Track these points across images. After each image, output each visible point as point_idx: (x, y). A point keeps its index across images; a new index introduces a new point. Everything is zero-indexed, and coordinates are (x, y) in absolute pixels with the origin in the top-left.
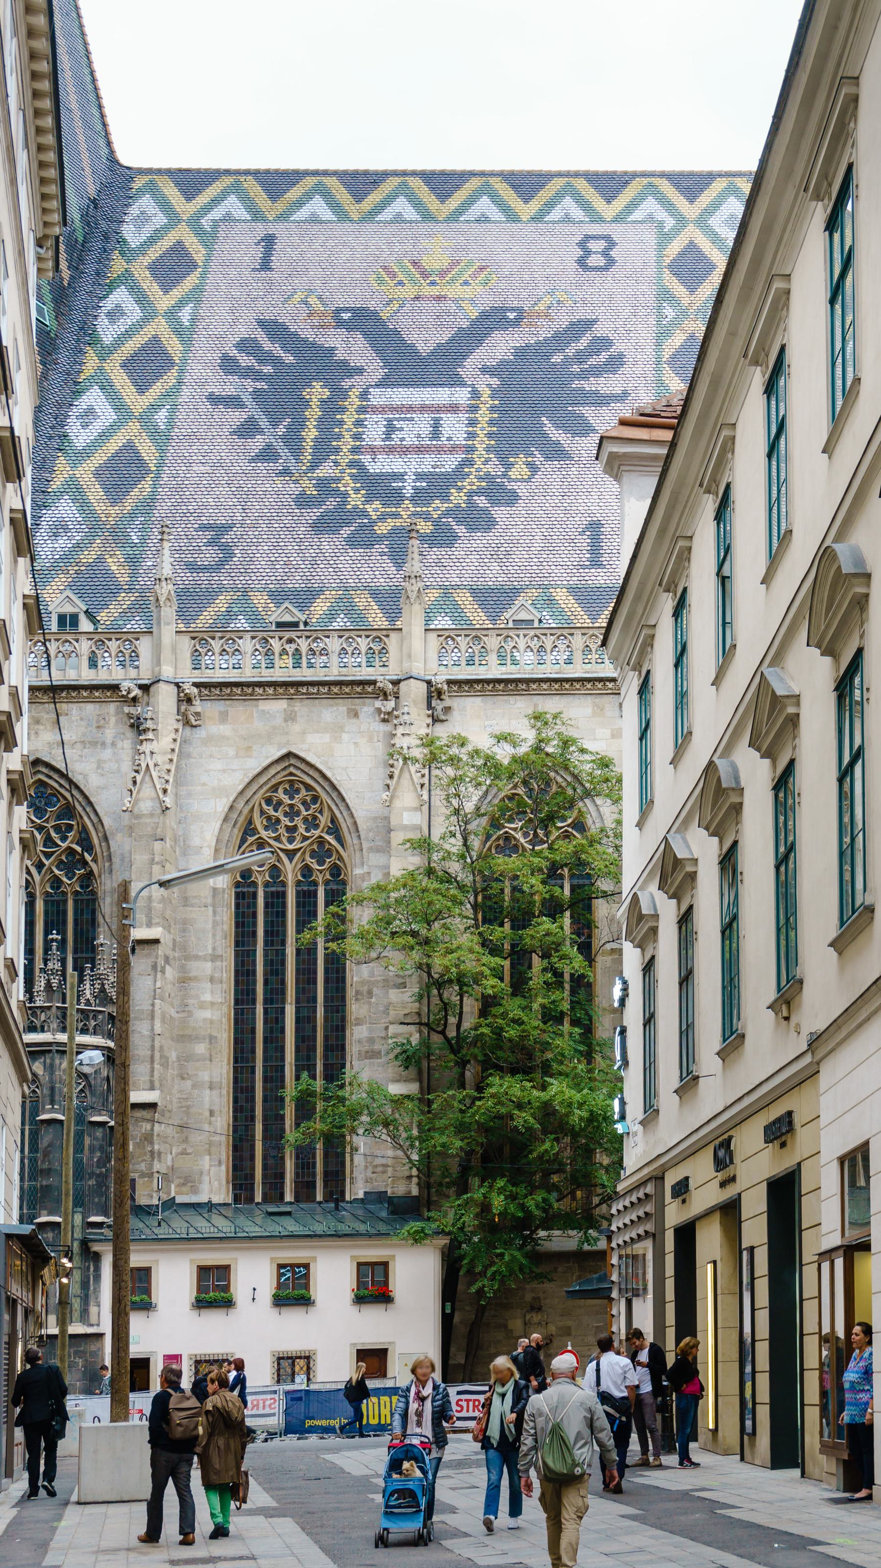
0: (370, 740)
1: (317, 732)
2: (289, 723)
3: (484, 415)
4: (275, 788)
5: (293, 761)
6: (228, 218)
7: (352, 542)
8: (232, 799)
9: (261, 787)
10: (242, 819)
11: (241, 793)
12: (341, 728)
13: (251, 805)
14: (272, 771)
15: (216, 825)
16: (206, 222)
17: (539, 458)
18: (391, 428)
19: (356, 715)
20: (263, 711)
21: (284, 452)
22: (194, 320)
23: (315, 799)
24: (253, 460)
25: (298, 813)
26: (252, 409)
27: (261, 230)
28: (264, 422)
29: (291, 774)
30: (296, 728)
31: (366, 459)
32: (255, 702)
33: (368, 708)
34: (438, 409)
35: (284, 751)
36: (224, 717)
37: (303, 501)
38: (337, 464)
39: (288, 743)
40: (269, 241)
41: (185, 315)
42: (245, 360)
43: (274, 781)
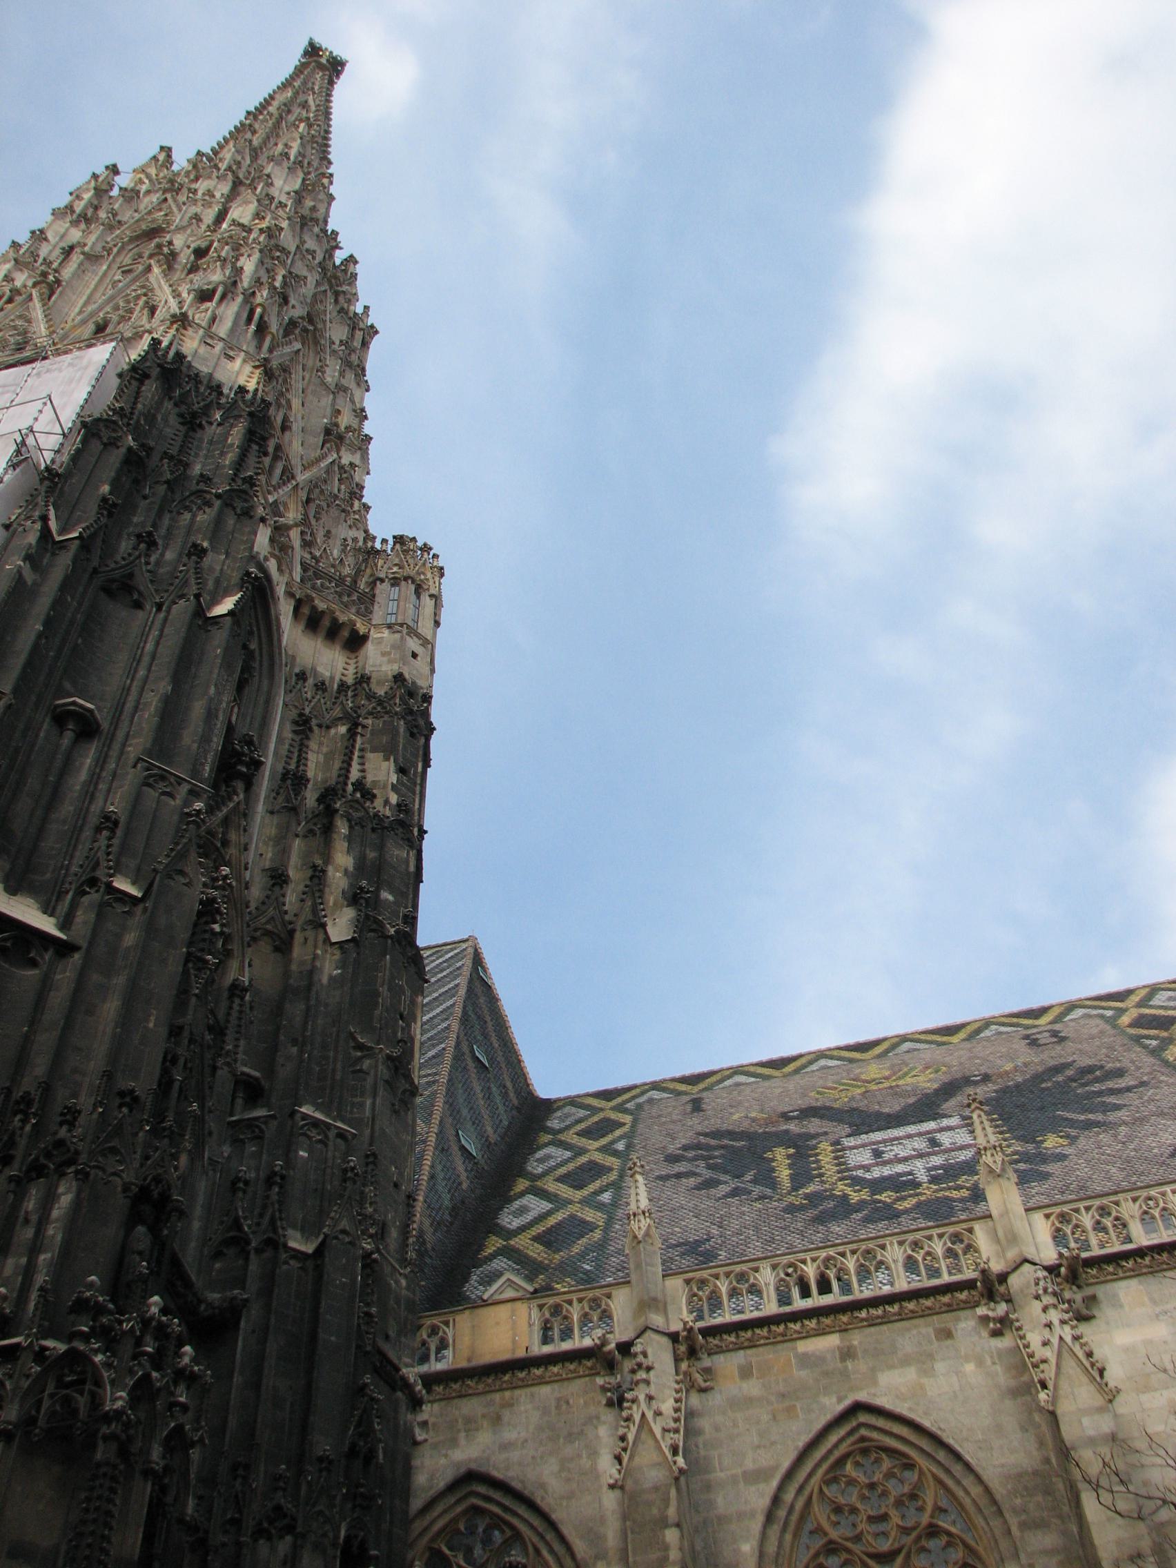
0: (980, 1363)
1: (891, 1367)
2: (849, 1364)
4: (841, 1462)
5: (863, 1418)
6: (650, 1101)
7: (867, 1220)
8: (775, 1483)
9: (818, 1465)
10: (794, 1517)
12: (931, 1356)
13: (806, 1492)
14: (833, 1438)
15: (756, 1525)
16: (628, 1106)
17: (1073, 1132)
18: (877, 1154)
19: (947, 1334)
20: (805, 1355)
21: (757, 1190)
22: (629, 1146)
23: (910, 1466)
24: (720, 1199)
25: (885, 1494)
26: (708, 1174)
28: (723, 1178)
30: (858, 1367)
31: (860, 1173)
32: (789, 1344)
33: (965, 1324)
35: (847, 1402)
36: (746, 1372)
37: (791, 1209)
38: (822, 1182)
39: (852, 1389)
41: (620, 1146)
42: (691, 1154)
43: (837, 1454)
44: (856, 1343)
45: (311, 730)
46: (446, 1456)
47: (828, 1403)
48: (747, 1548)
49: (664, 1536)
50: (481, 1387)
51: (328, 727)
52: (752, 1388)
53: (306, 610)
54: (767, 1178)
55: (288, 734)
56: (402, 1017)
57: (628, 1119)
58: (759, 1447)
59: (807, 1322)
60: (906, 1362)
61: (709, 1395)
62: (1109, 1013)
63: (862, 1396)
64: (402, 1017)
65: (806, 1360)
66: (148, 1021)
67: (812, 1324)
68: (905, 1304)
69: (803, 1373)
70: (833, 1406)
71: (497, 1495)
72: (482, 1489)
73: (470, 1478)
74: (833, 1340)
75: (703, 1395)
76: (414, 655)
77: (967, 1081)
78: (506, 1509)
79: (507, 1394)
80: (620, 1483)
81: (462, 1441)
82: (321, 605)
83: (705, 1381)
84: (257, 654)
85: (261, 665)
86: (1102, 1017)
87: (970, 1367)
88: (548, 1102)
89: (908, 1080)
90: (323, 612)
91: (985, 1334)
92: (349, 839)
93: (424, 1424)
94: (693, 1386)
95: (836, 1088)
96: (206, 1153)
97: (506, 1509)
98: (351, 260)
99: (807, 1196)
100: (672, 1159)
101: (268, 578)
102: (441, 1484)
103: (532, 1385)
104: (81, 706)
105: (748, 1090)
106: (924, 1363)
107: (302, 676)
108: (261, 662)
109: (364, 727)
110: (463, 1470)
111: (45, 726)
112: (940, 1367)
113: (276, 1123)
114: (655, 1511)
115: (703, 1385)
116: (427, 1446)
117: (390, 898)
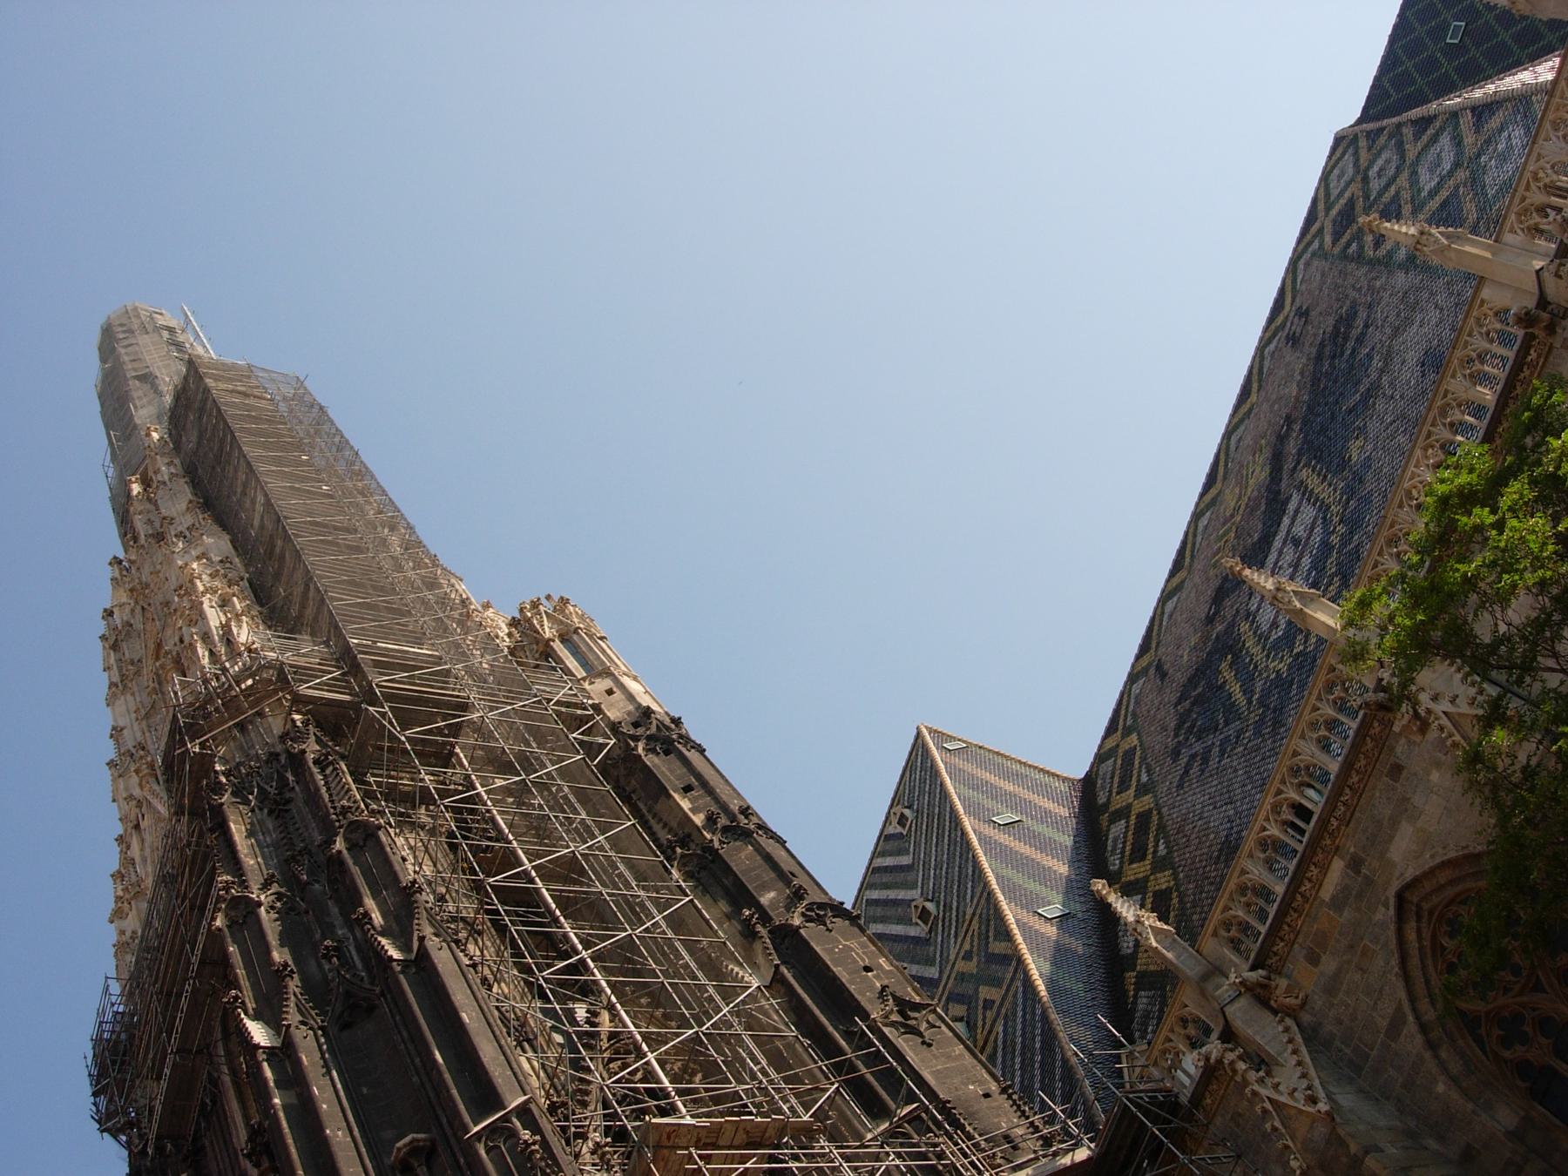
0: (1438, 765)
1: (1391, 838)
3: (1313, 481)
8: (1411, 1018)
11: (1412, 999)
12: (1406, 800)
16: (1129, 722)
20: (1333, 898)
21: (1231, 731)
27: (1152, 671)
29: (1431, 913)
34: (1288, 532)
35: (1392, 901)
36: (1314, 959)
40: (1159, 667)
41: (1144, 778)
44: (1352, 850)
47: (1381, 917)
48: (1441, 1088)
52: (1329, 964)
54: (1231, 710)
56: (867, 969)
57: (1134, 739)
58: (1376, 1003)
59: (1315, 860)
60: (1394, 823)
62: (1316, 245)
63: (1395, 886)
64: (867, 969)
65: (1338, 903)
67: (1314, 871)
68: (1350, 782)
69: (1347, 914)
70: (1385, 914)
74: (1338, 865)
75: (1307, 1007)
77: (1282, 439)
83: (1297, 997)
86: (1314, 254)
87: (1435, 776)
88: (1088, 775)
89: (1251, 482)
91: (1418, 738)
95: (1220, 548)
99: (1261, 703)
100: (1176, 754)
105: (1177, 615)
106: (1406, 810)
112: (1417, 800)
114: (1344, 1160)
115: (1298, 1002)
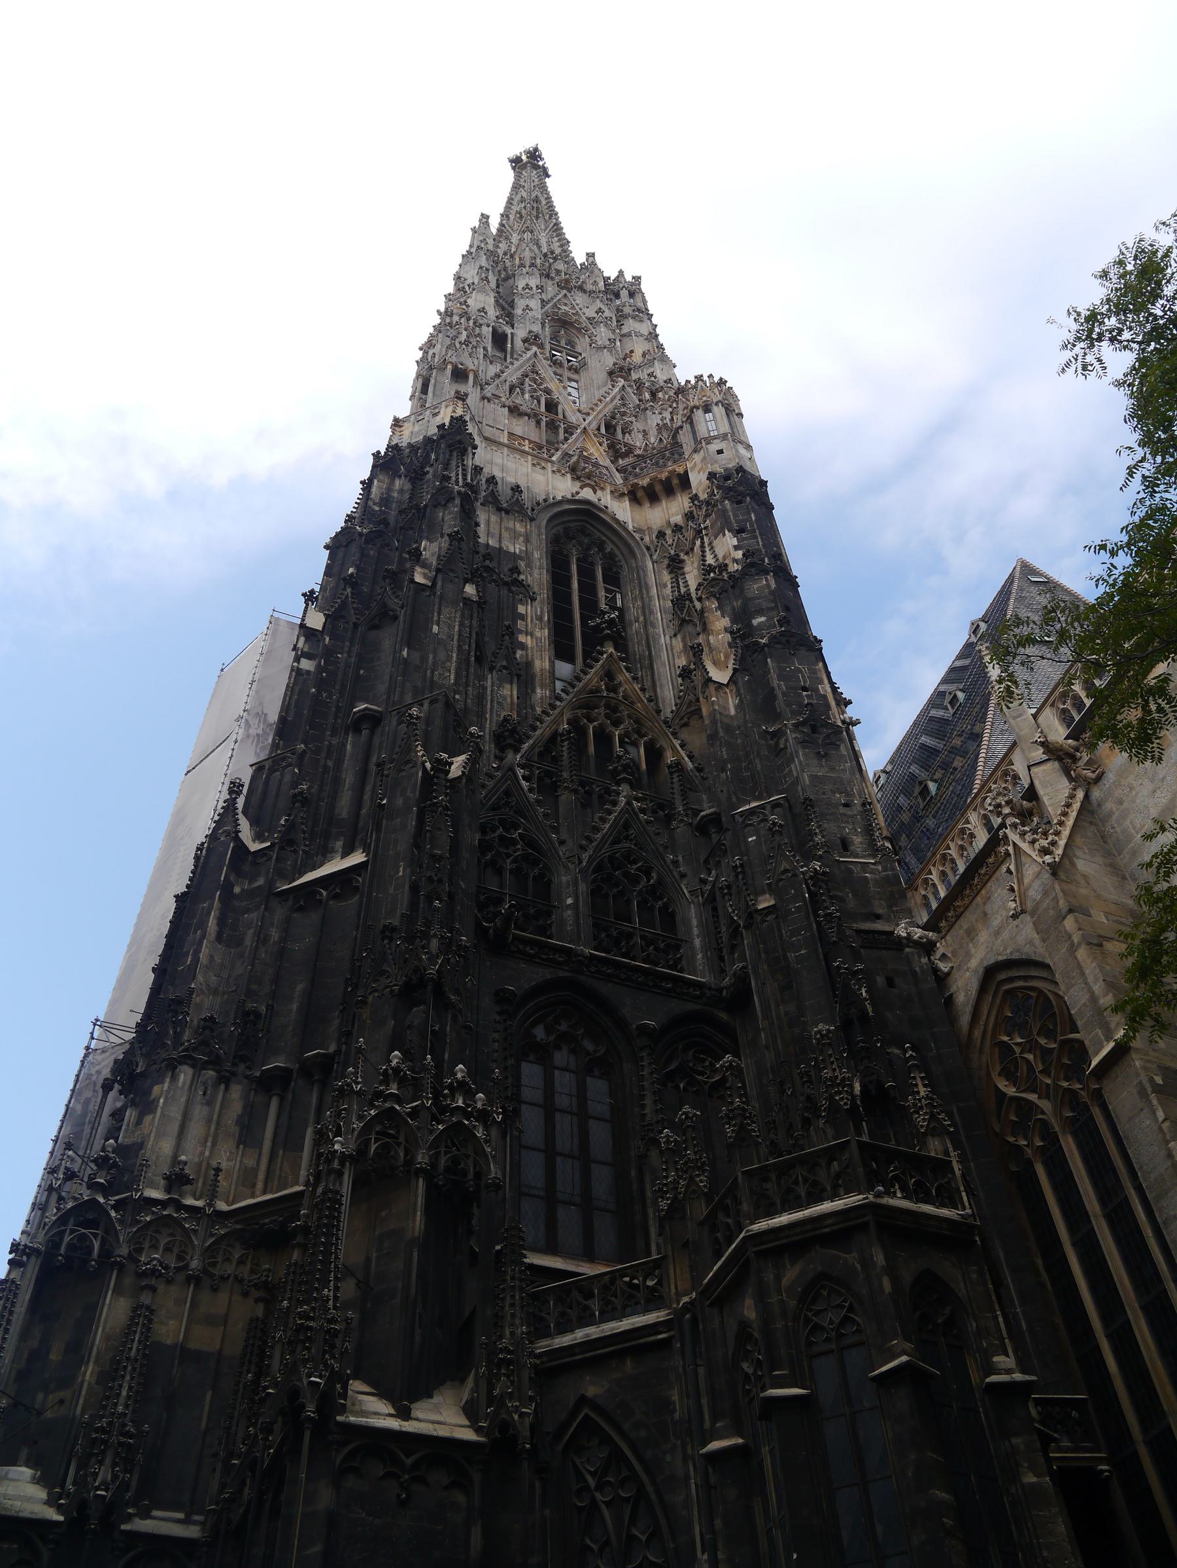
45: (683, 561)
46: (968, 969)
49: (1065, 927)
50: (966, 901)
51: (692, 549)
53: (640, 494)
55: (666, 577)
56: (805, 689)
61: (1104, 781)
66: (398, 872)
71: (1014, 973)
72: (1003, 976)
73: (990, 972)
75: (1100, 783)
76: (720, 452)
78: (1025, 978)
79: (983, 892)
80: (1019, 909)
81: (973, 951)
82: (645, 482)
84: (616, 551)
85: (623, 555)
90: (651, 485)
92: (720, 608)
93: (944, 957)
94: (1089, 783)
96: (685, 891)
97: (1025, 978)
98: (591, 255)
101: (587, 502)
102: (973, 993)
103: (994, 872)
104: (359, 711)
107: (661, 535)
108: (622, 553)
109: (705, 528)
110: (981, 971)
111: (350, 739)
113: (730, 832)
115: (1093, 776)
116: (955, 973)
117: (763, 619)
